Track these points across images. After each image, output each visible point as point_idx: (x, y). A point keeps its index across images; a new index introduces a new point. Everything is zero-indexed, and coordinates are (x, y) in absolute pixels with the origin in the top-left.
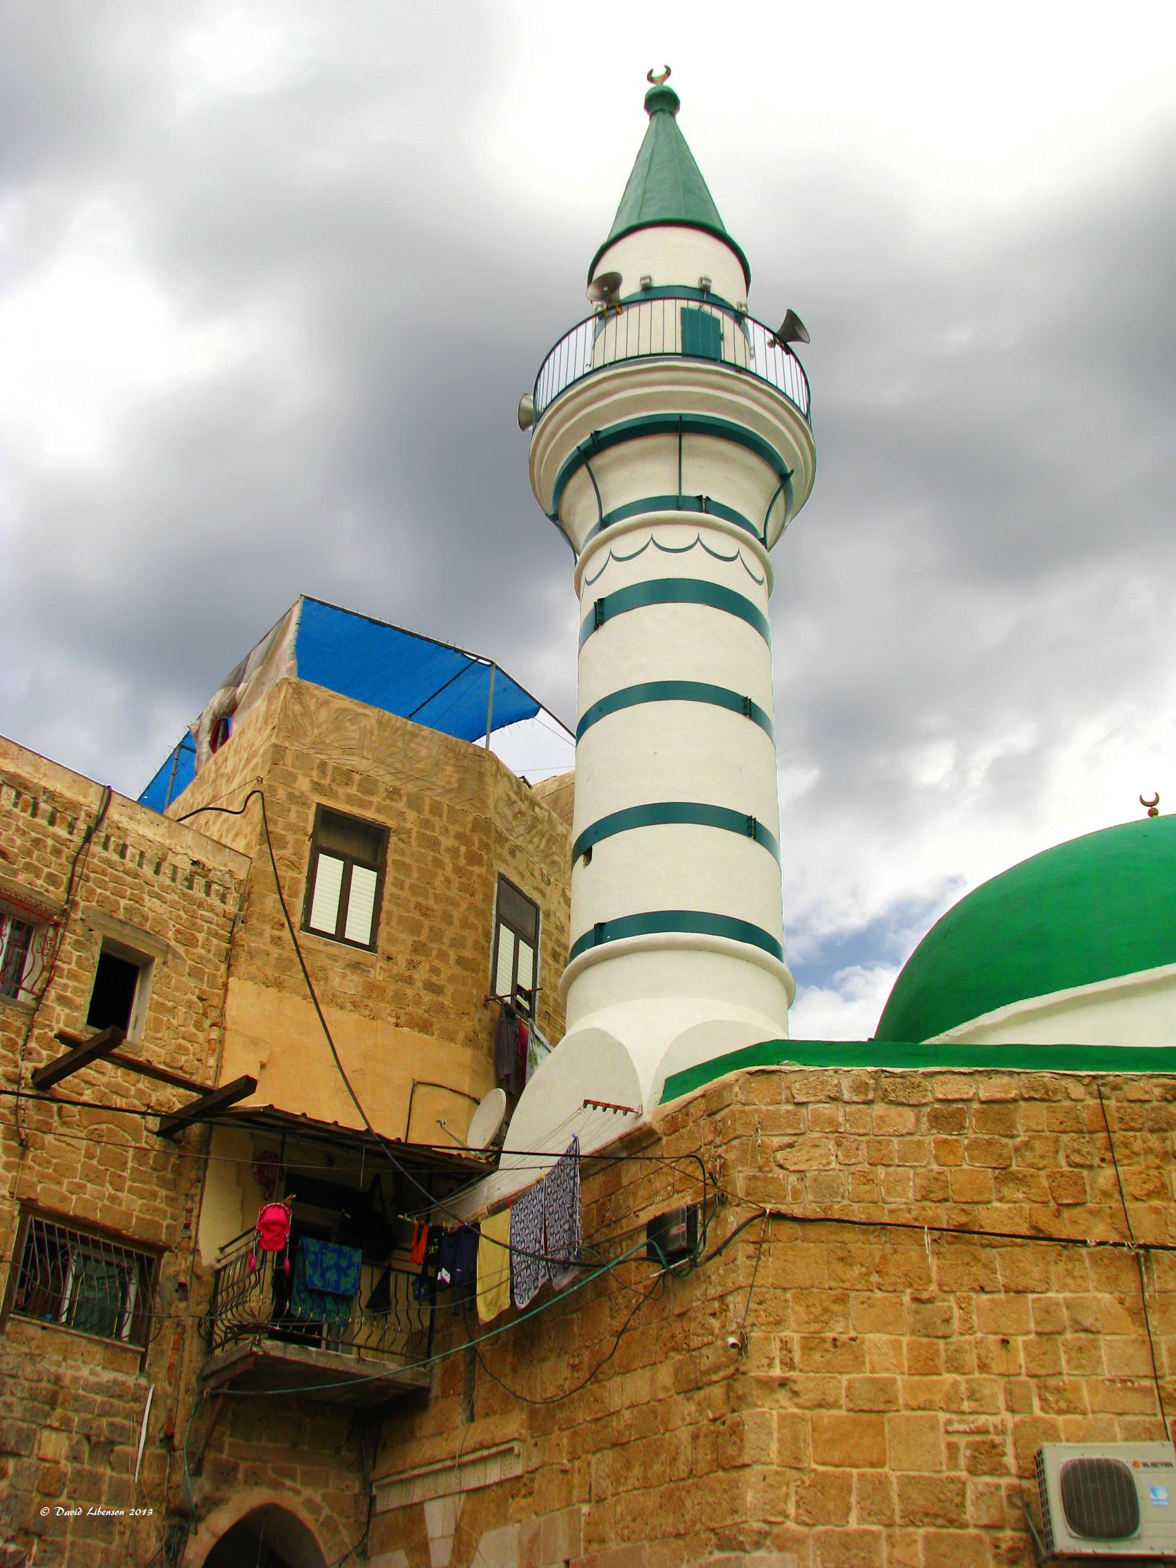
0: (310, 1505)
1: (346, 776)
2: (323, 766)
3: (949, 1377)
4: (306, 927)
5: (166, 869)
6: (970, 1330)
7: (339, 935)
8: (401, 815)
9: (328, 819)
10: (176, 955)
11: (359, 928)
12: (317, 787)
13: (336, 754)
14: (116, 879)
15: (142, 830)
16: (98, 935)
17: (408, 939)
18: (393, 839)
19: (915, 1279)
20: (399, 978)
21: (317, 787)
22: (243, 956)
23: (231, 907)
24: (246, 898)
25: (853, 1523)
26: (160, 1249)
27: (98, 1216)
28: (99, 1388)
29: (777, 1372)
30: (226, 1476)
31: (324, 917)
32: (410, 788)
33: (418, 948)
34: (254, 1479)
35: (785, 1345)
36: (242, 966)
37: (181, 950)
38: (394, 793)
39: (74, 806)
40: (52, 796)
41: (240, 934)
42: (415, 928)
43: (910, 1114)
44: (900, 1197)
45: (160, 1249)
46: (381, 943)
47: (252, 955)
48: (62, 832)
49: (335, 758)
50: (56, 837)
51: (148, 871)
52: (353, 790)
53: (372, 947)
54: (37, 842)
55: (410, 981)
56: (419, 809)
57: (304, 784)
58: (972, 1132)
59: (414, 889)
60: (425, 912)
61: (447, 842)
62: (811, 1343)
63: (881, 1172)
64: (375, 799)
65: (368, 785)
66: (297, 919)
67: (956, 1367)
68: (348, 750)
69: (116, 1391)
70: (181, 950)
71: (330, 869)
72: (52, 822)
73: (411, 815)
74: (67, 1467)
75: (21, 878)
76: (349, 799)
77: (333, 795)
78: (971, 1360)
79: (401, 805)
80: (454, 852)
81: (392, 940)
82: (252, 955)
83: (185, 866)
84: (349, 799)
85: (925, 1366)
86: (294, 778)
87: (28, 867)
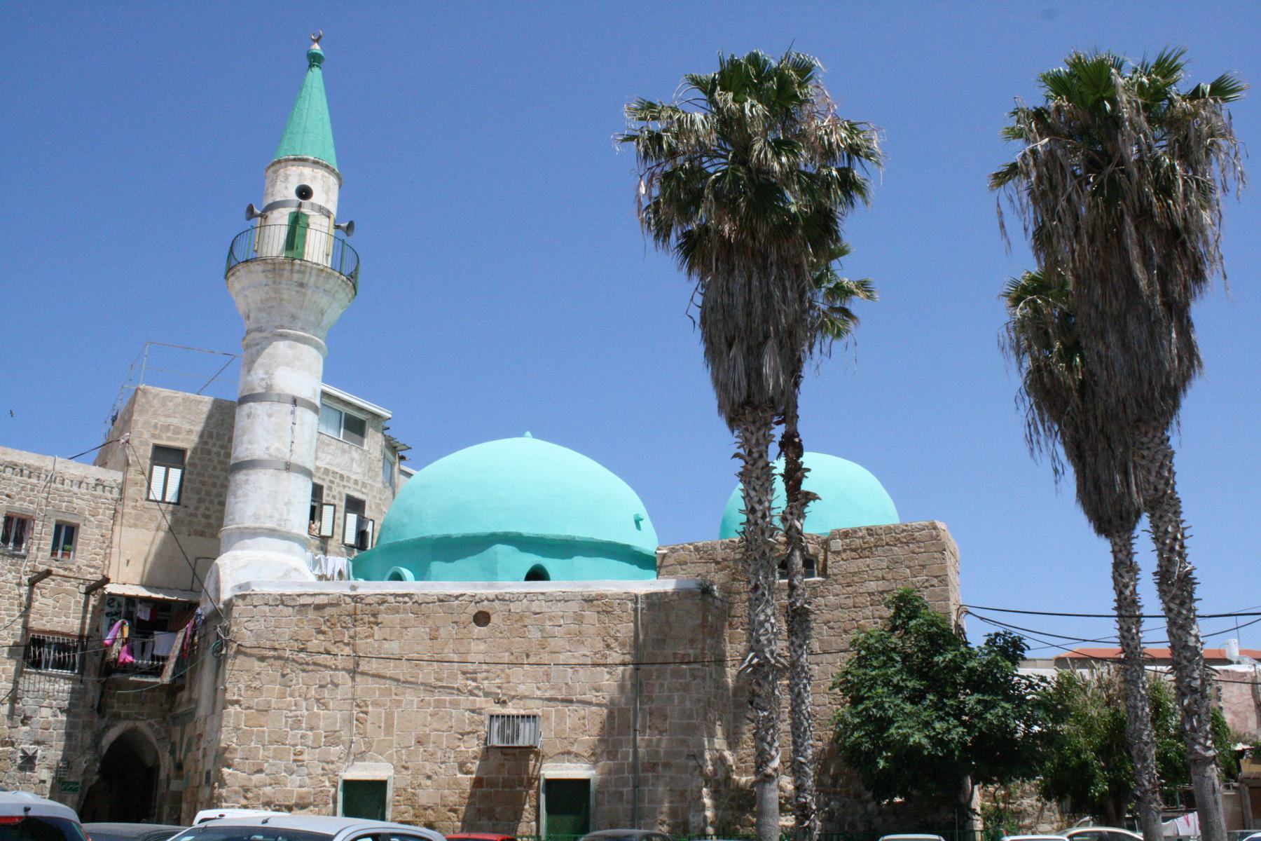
0: (150, 725)
1: (167, 428)
2: (155, 426)
3: (289, 699)
4: (148, 499)
5: (84, 485)
7: (163, 501)
11: (171, 496)
12: (153, 436)
13: (162, 419)
15: (71, 471)
16: (53, 521)
17: (195, 497)
20: (191, 515)
23: (116, 494)
24: (122, 491)
25: (253, 745)
27: (59, 629)
29: (235, 698)
30: (117, 717)
31: (156, 493)
33: (200, 500)
34: (127, 717)
35: (239, 689)
39: (39, 468)
40: (29, 466)
41: (119, 508)
42: (198, 492)
46: (183, 501)
48: (34, 481)
49: (162, 421)
50: (31, 484)
51: (75, 489)
52: (169, 434)
53: (178, 503)
54: (23, 489)
55: (196, 515)
57: (146, 435)
59: (198, 474)
60: (203, 483)
61: (215, 450)
62: (248, 687)
65: (177, 431)
66: (144, 496)
67: (292, 695)
71: (159, 471)
72: (30, 477)
74: (51, 719)
75: (17, 504)
76: (169, 439)
77: (159, 437)
78: (297, 694)
80: (218, 454)
81: (188, 498)
83: (93, 482)
84: (169, 439)
85: (282, 696)
87: (21, 499)
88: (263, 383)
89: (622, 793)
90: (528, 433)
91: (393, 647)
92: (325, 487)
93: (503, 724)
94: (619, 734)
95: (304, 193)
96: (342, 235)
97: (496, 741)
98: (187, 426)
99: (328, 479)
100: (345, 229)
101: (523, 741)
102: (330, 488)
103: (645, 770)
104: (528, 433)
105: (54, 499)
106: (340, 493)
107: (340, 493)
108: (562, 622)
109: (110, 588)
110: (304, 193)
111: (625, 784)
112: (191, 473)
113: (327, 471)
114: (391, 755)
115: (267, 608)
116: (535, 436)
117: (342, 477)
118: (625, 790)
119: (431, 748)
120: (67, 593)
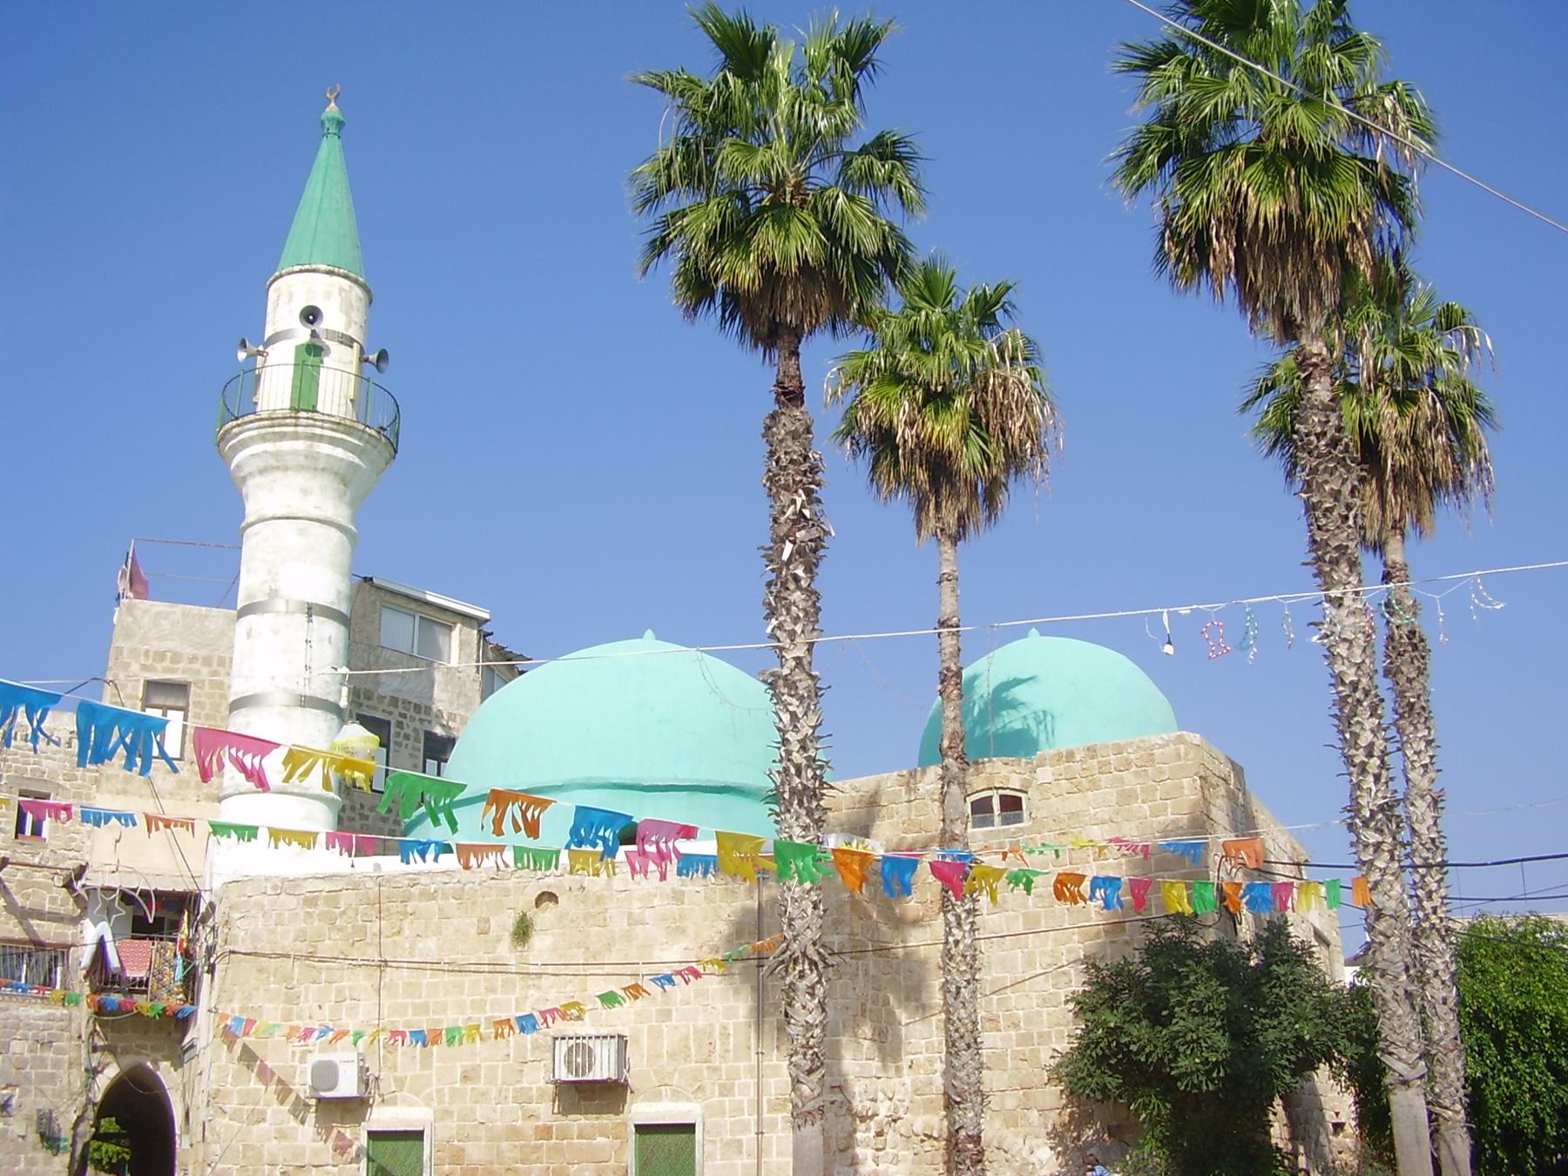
1: (161, 656)
6: (307, 1001)
8: (198, 672)
9: (151, 685)
10: (64, 788)
12: (144, 667)
14: (23, 756)
18: (193, 688)
19: (287, 978)
21: (144, 667)
22: (103, 780)
26: (69, 947)
28: (40, 1019)
32: (203, 653)
36: (104, 786)
37: (68, 785)
38: (194, 659)
43: (294, 900)
44: (287, 943)
45: (69, 947)
47: (108, 778)
49: (155, 645)
52: (167, 663)
56: (210, 665)
57: (135, 667)
58: (322, 907)
63: (280, 928)
64: (181, 666)
65: (176, 658)
68: (163, 638)
69: (49, 1018)
70: (68, 785)
73: (205, 671)
74: (27, 1055)
76: (165, 670)
79: (197, 666)
82: (108, 778)
84: (165, 670)
86: (128, 665)
88: (266, 588)
89: (740, 1142)
90: (649, 633)
91: (428, 948)
92: (393, 722)
93: (570, 1049)
94: (736, 1060)
95: (311, 315)
96: (371, 370)
97: (563, 1075)
98: (190, 651)
99: (396, 712)
100: (375, 361)
101: (603, 1070)
102: (400, 725)
103: (773, 1109)
104: (649, 633)
105: (16, 761)
106: (415, 730)
107: (415, 730)
108: (656, 902)
109: (93, 879)
110: (311, 315)
111: (746, 1129)
112: (197, 716)
113: (394, 701)
114: (430, 1094)
115: (265, 900)
116: (659, 637)
117: (417, 708)
118: (744, 1138)
119: (482, 1085)
120: (39, 885)
